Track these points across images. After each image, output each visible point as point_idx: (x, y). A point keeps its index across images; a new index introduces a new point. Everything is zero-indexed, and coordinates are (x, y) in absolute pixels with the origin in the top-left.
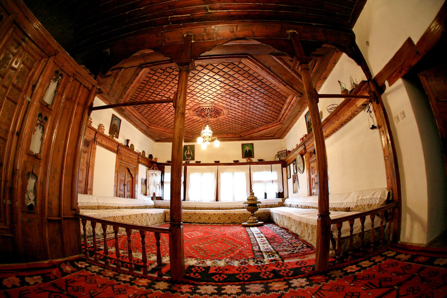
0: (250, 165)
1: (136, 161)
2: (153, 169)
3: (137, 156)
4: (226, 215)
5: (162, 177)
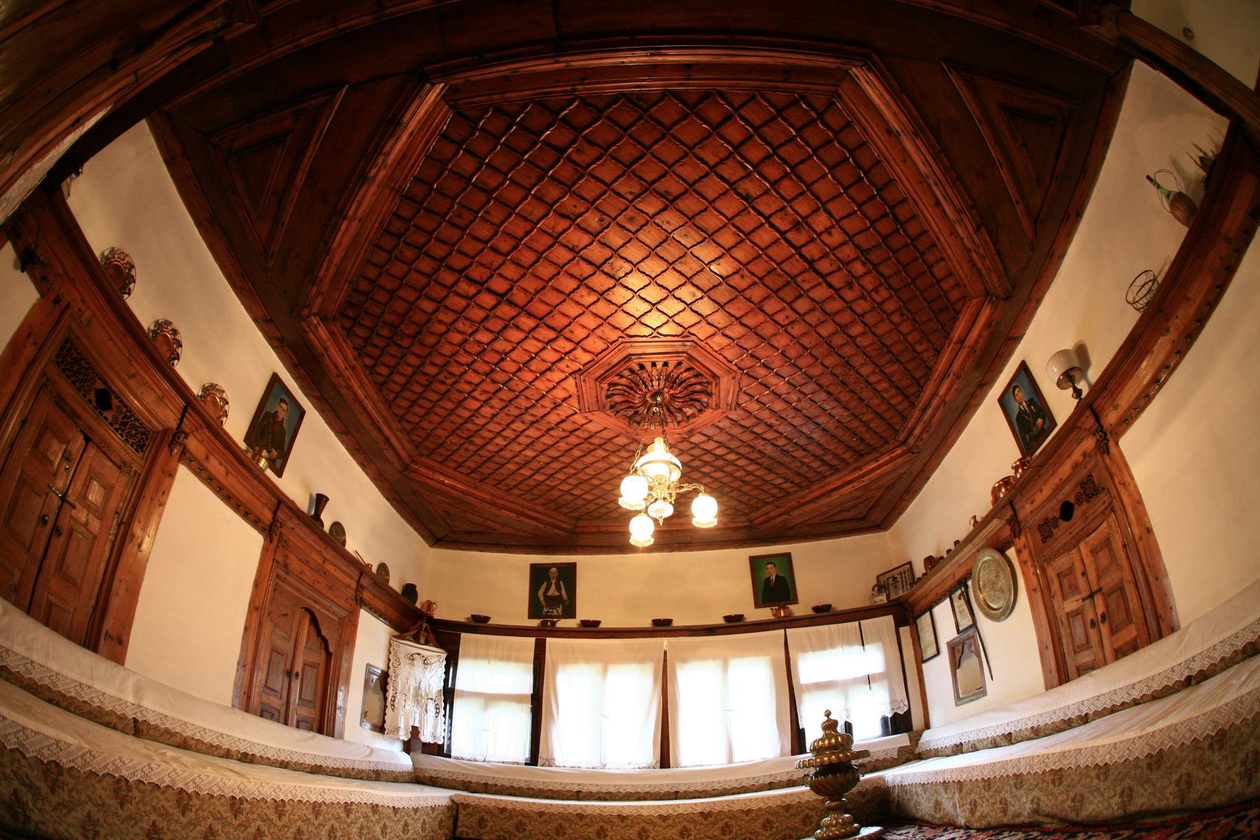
0: (785, 628)
1: (351, 593)
2: (416, 639)
3: (356, 574)
5: (447, 673)
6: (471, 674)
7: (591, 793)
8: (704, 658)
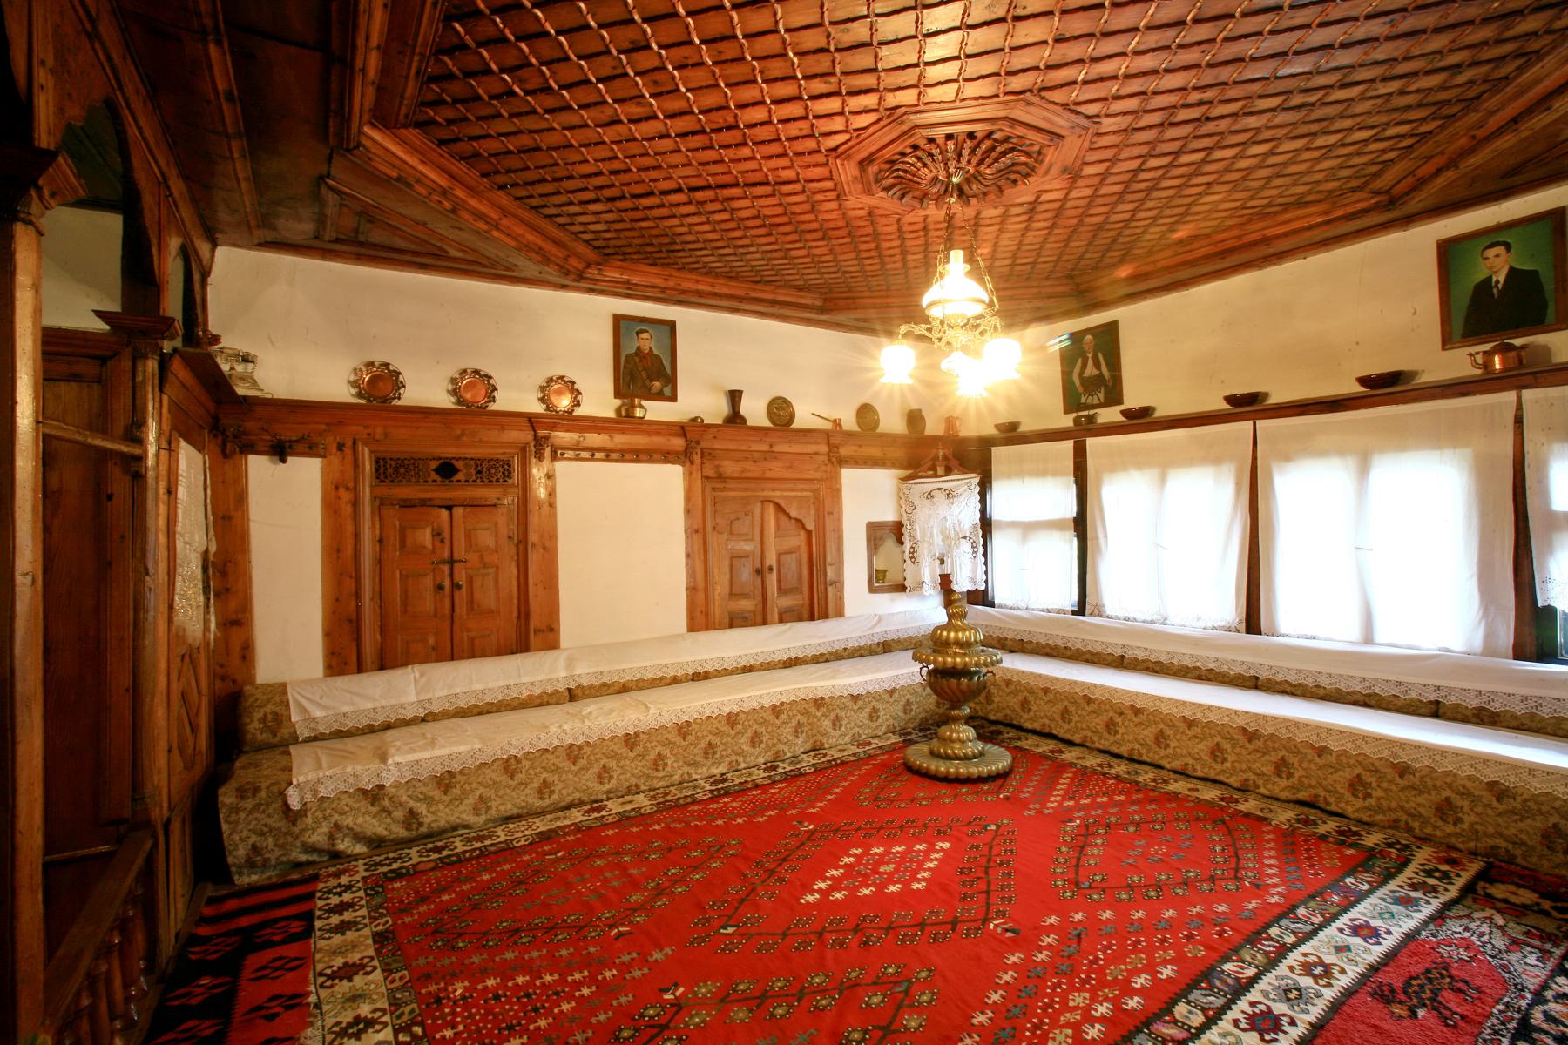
4: (1259, 744)
6: (1009, 499)
7: (1136, 659)
8: (1322, 453)
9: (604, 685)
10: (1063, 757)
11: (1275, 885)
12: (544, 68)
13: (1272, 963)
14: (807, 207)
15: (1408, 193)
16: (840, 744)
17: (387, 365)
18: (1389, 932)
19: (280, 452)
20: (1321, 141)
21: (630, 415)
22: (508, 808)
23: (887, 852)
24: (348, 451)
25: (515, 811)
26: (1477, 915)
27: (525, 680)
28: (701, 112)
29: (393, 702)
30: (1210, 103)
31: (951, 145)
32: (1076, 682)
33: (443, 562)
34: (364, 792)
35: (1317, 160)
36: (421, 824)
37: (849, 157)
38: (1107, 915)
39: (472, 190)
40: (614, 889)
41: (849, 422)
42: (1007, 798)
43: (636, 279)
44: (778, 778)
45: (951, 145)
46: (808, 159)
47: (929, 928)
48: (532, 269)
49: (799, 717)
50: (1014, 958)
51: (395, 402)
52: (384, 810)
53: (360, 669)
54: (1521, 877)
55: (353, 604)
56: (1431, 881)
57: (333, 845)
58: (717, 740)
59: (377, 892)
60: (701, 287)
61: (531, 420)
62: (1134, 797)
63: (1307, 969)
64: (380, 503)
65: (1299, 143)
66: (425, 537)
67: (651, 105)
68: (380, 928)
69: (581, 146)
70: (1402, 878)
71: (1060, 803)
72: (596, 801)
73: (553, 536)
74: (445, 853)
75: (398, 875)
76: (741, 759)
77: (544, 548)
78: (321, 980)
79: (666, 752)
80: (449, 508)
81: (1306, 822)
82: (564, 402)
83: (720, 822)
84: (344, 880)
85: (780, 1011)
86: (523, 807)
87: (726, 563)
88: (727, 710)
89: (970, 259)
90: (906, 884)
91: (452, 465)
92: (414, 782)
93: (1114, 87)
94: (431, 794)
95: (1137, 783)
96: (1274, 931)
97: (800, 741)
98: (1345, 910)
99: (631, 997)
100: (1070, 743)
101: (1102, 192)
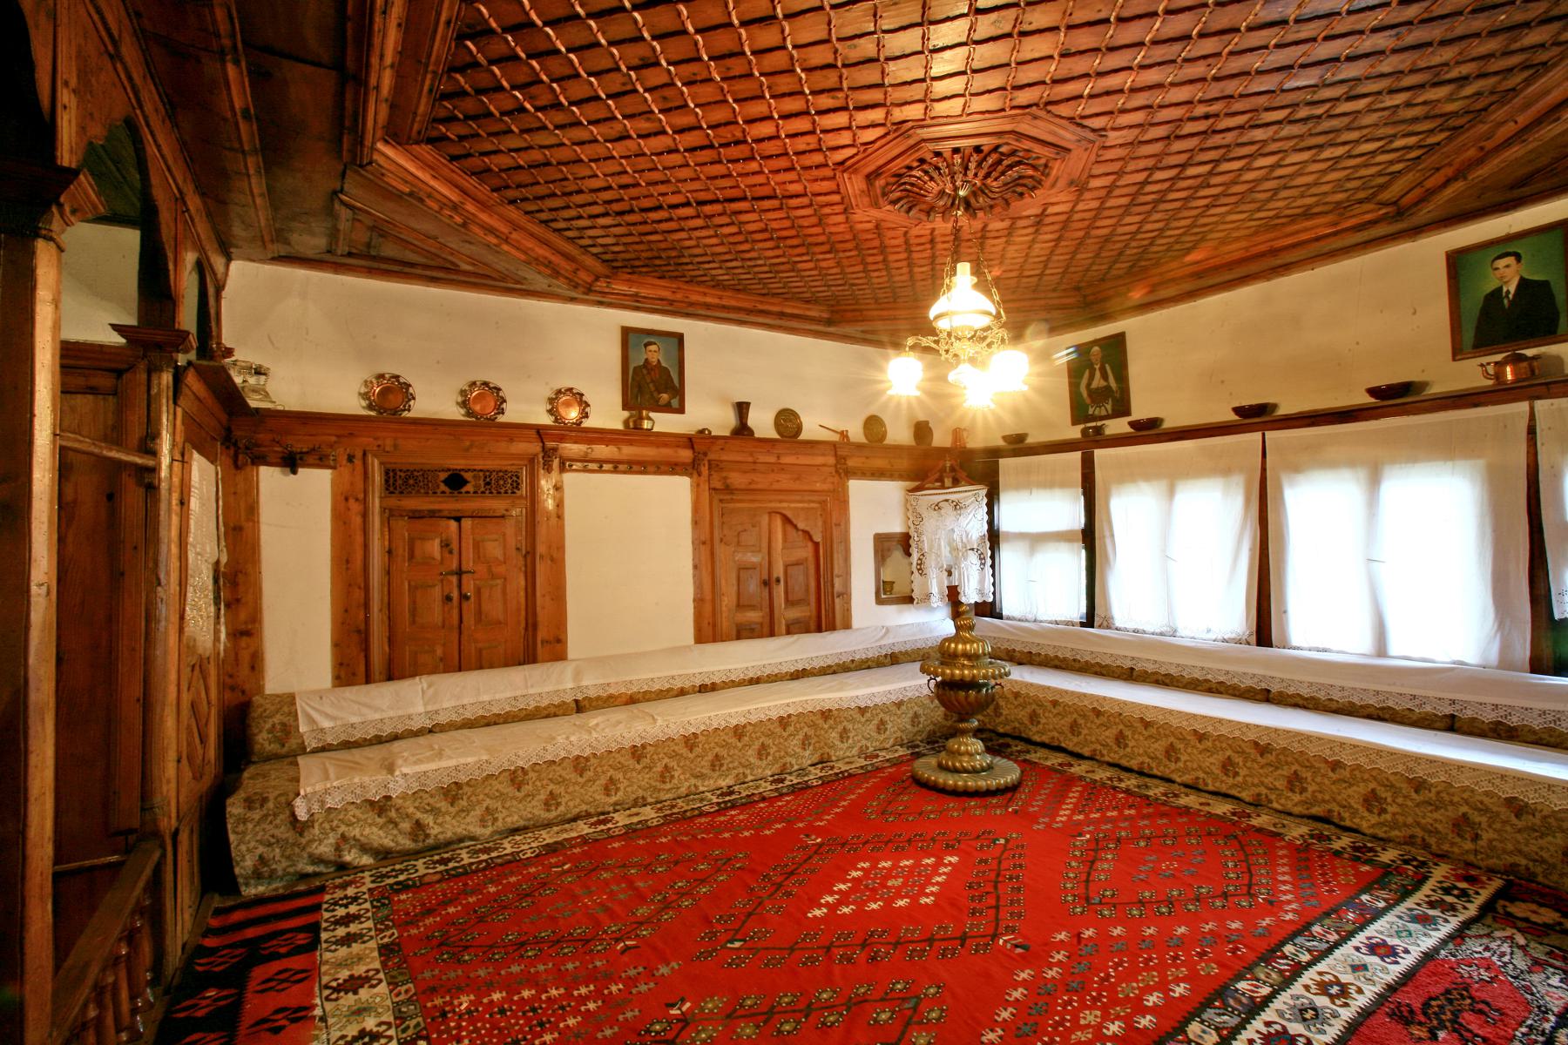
4: (1270, 758)
6: (1016, 511)
7: (1146, 672)
8: (1332, 464)
9: (611, 696)
10: (1072, 770)
11: (1289, 902)
12: (555, 85)
13: (1287, 982)
14: (814, 220)
15: (1416, 204)
16: (847, 756)
17: (397, 377)
18: (1407, 951)
19: (291, 463)
20: (1327, 154)
21: (638, 427)
22: (515, 820)
23: (895, 866)
24: (358, 462)
25: (522, 823)
26: (1497, 934)
27: (531, 691)
28: (709, 127)
29: (401, 713)
30: (1216, 115)
31: (957, 159)
32: (1085, 695)
33: (451, 573)
34: (371, 803)
35: (1324, 172)
36: (427, 836)
37: (856, 171)
38: (1118, 931)
39: (483, 205)
40: (620, 902)
41: (856, 433)
42: (1015, 812)
43: (644, 292)
44: (785, 791)
45: (957, 159)
46: (815, 173)
47: (936, 943)
48: (541, 282)
49: (806, 729)
50: (1024, 975)
51: (405, 414)
52: (391, 821)
53: (368, 680)
54: (1542, 895)
55: (362, 616)
56: (1449, 899)
57: (340, 856)
58: (723, 752)
59: (384, 904)
60: (709, 300)
61: (540, 432)
62: (1145, 811)
63: (1323, 988)
64: (390, 515)
65: (1305, 156)
66: (434, 548)
67: (660, 120)
68: (386, 940)
69: (591, 161)
70: (1419, 896)
71: (1070, 817)
72: (603, 814)
73: (561, 548)
74: (451, 865)
75: (404, 887)
76: (748, 772)
77: (552, 560)
78: (326, 992)
79: (673, 764)
80: (458, 519)
81: (1320, 837)
82: (573, 414)
83: (726, 835)
84: (351, 891)
85: (787, 1027)
86: (529, 820)
87: (734, 575)
88: (734, 722)
89: (976, 272)
90: (915, 899)
91: (462, 477)
92: (421, 794)
93: (1120, 101)
94: (438, 805)
95: (1147, 797)
96: (1288, 949)
97: (807, 753)
98: (1361, 928)
99: (637, 1012)
100: (1079, 756)
101: (1108, 204)
